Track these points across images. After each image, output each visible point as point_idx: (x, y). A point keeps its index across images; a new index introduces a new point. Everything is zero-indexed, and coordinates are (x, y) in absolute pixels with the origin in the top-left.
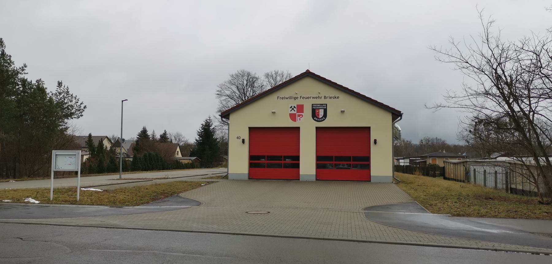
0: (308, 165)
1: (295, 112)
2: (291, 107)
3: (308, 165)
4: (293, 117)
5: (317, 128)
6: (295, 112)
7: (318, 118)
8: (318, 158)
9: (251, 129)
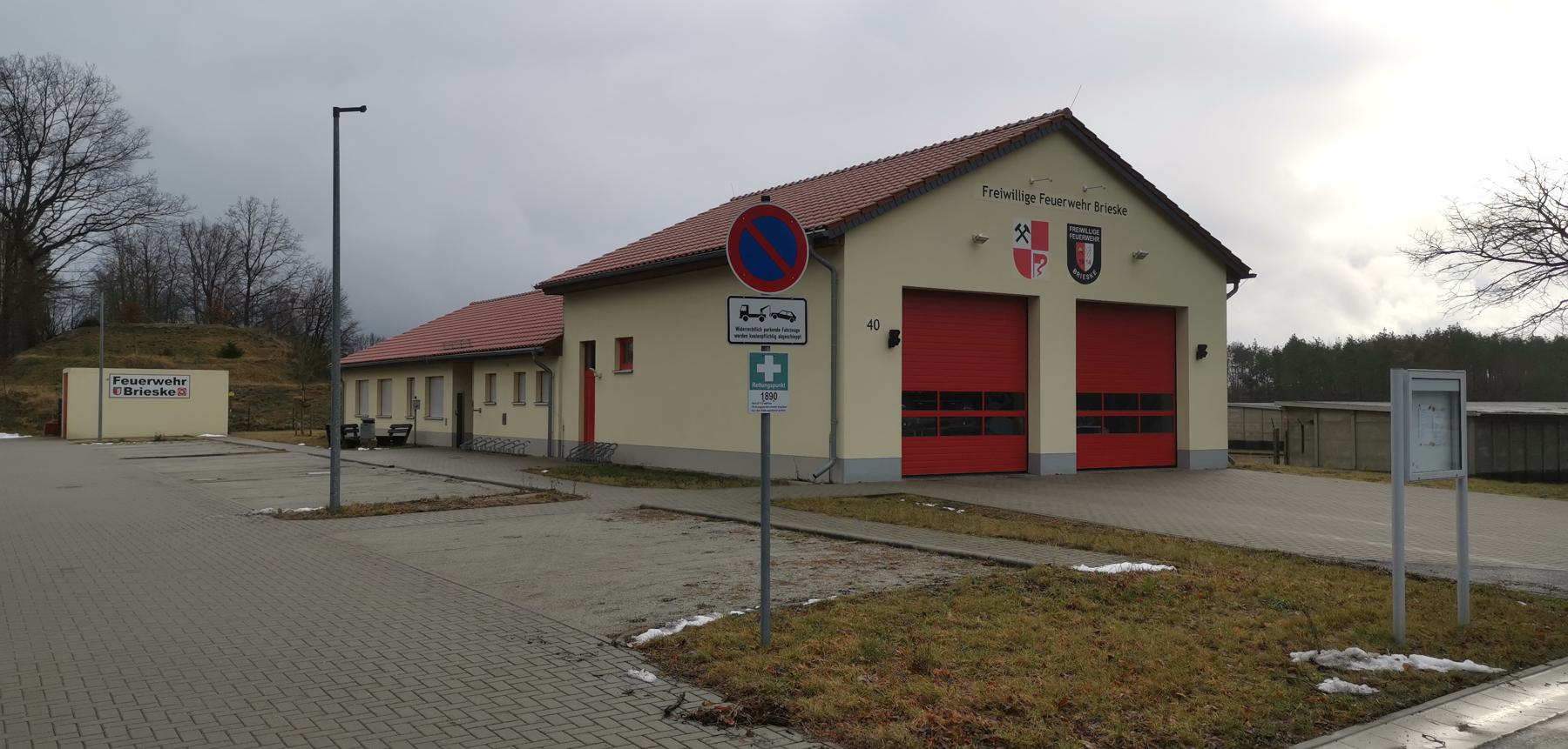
0: (1055, 425)
1: (1028, 246)
2: (1018, 228)
3: (1055, 425)
4: (1023, 262)
5: (1081, 304)
6: (1028, 246)
7: (1082, 272)
9: (910, 294)
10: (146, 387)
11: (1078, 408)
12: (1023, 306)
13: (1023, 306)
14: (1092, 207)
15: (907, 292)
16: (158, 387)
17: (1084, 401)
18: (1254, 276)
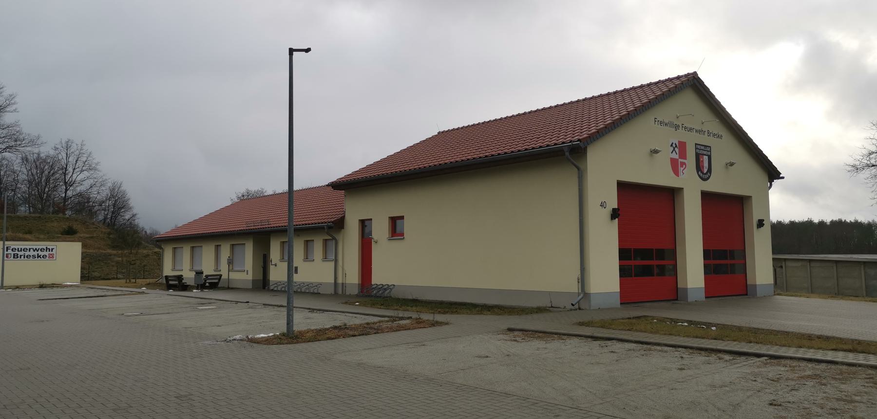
0: (693, 272)
1: (677, 157)
3: (693, 272)
4: (675, 166)
7: (702, 173)
8: (624, 254)
9: (622, 186)
10: (27, 253)
12: (672, 194)
13: (672, 194)
16: (36, 253)
18: (783, 178)
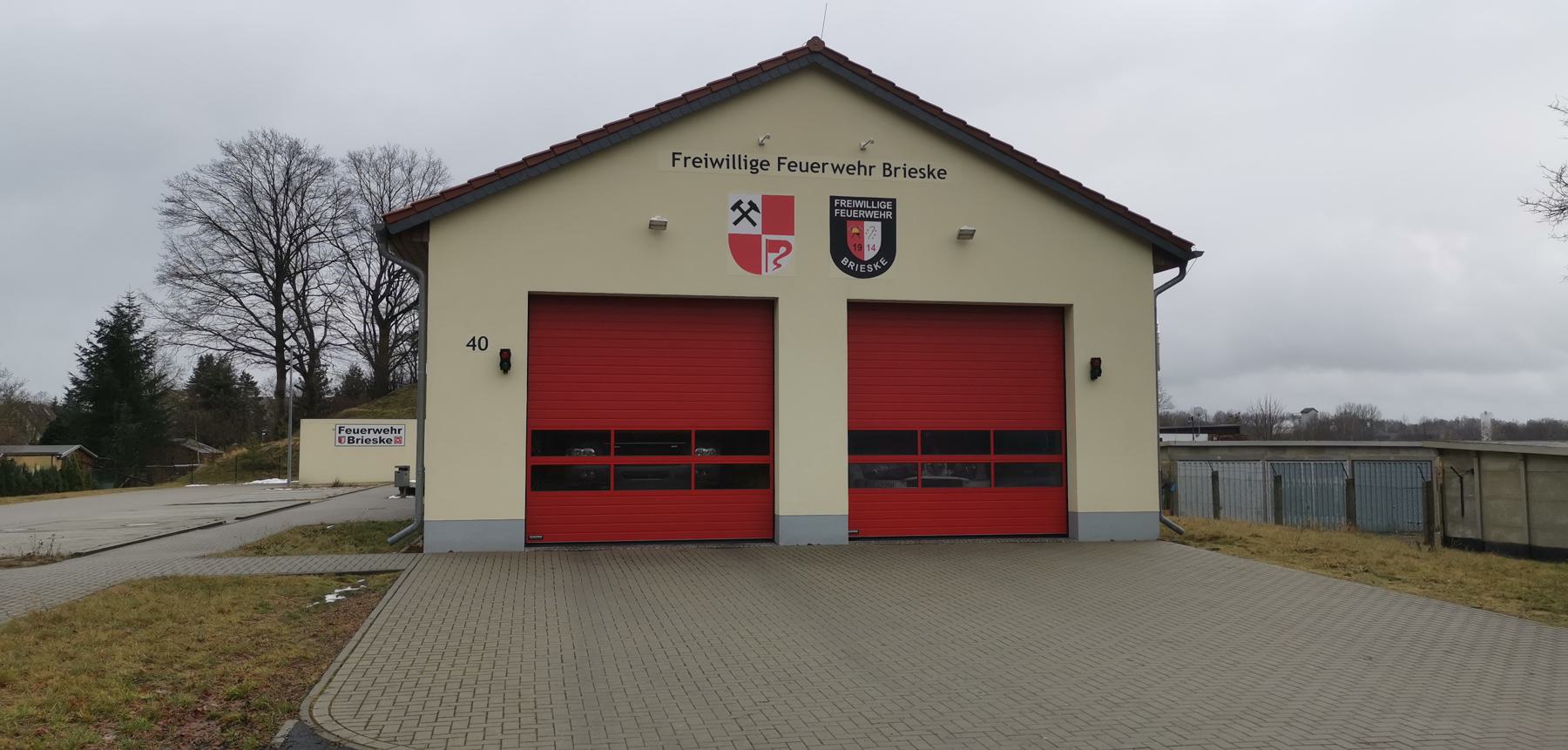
1: (757, 230)
2: (737, 206)
4: (746, 252)
5: (855, 307)
6: (757, 230)
7: (859, 261)
8: (859, 442)
9: (538, 301)
10: (366, 436)
11: (850, 453)
12: (760, 314)
13: (760, 314)
14: (900, 172)
15: (536, 299)
16: (377, 436)
17: (862, 442)
18: (1200, 254)
